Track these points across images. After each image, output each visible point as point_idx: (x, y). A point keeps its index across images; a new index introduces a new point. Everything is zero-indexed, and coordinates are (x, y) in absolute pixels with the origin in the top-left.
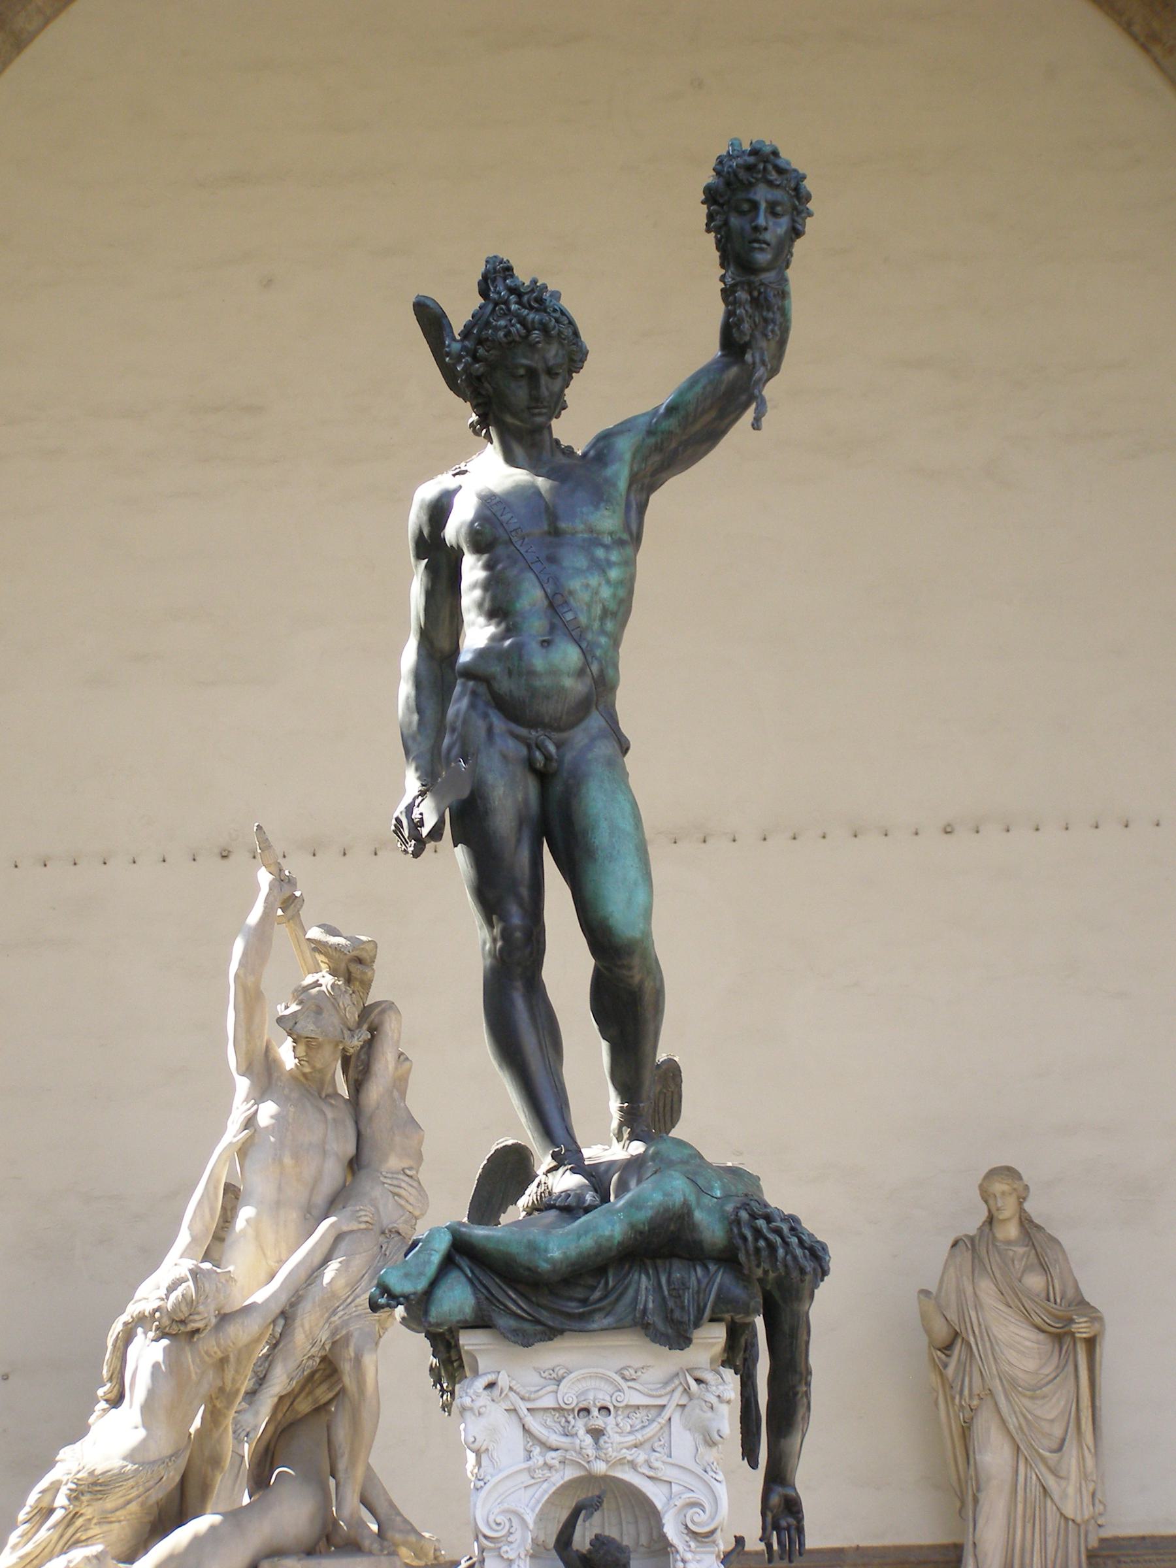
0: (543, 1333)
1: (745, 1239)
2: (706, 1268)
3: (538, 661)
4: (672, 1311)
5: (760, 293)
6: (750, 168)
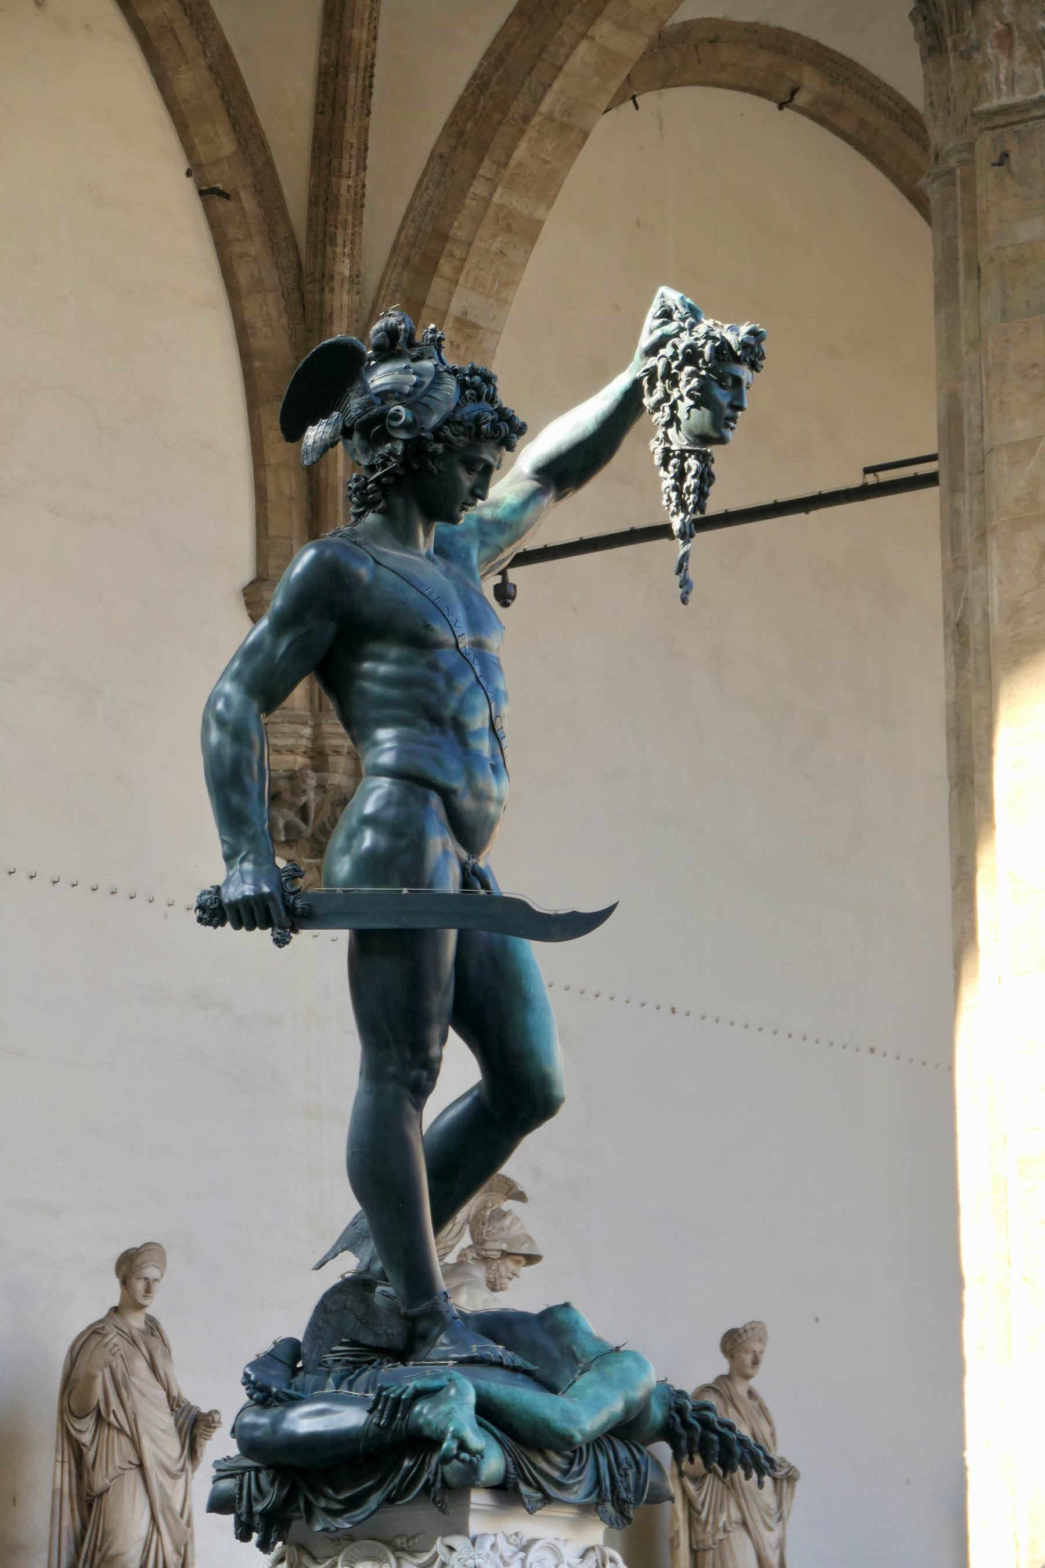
0: (541, 1501)
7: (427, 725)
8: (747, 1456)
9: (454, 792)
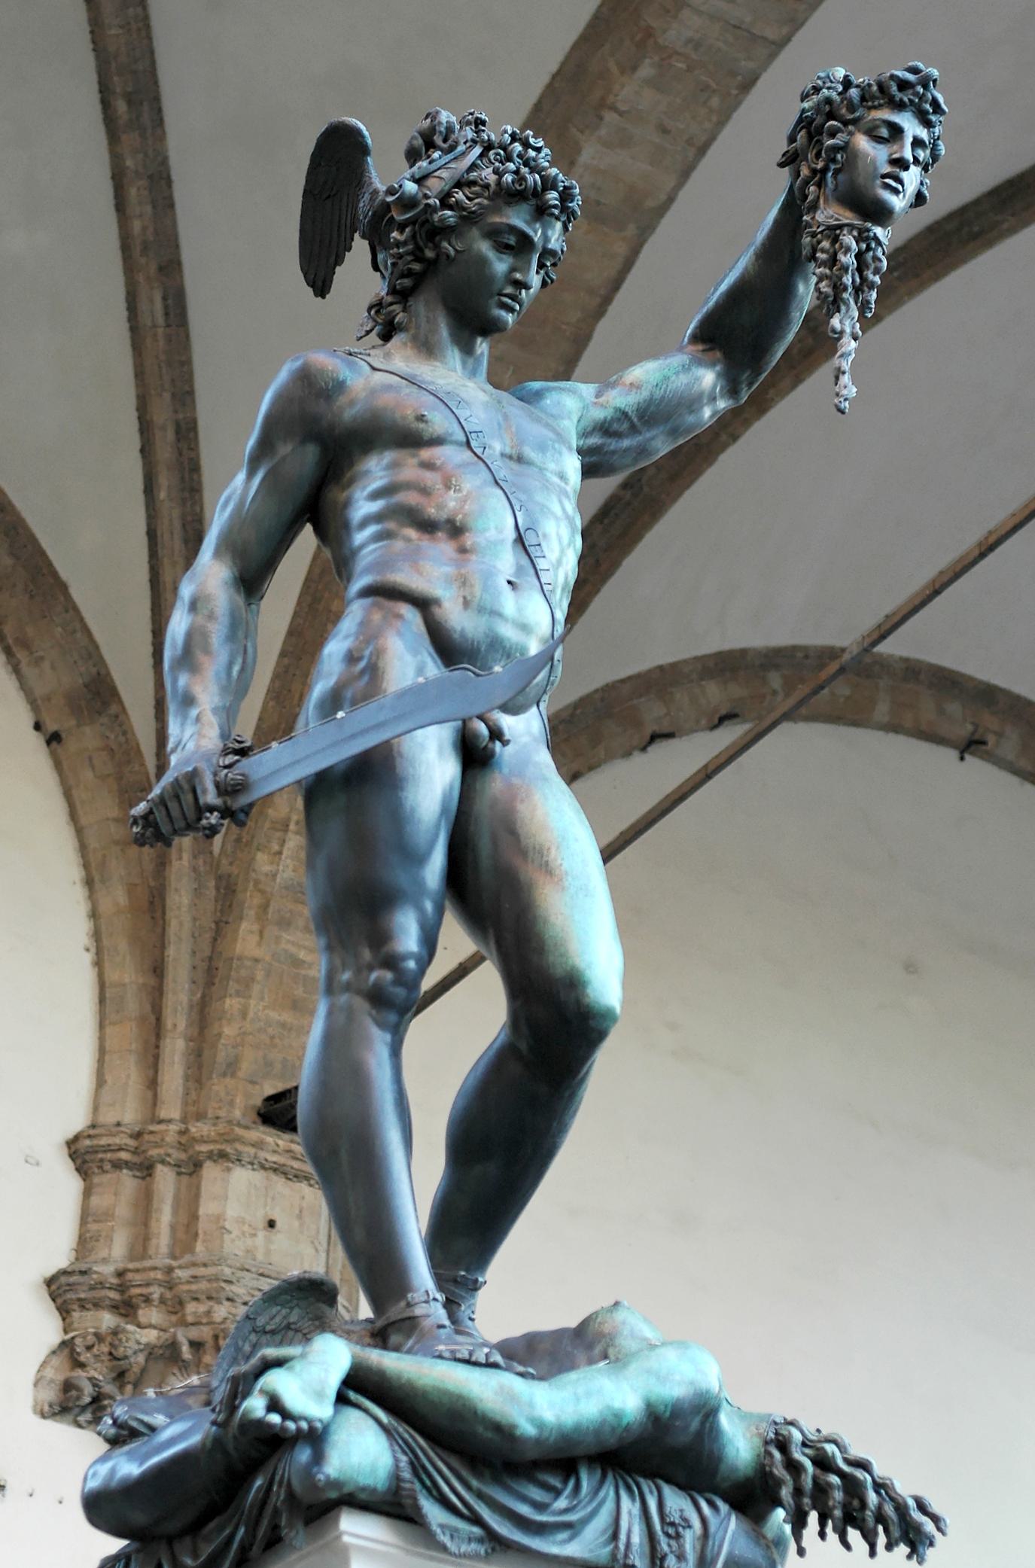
0: (480, 1541)
1: (794, 1467)
2: (712, 1504)
3: (509, 603)
4: (663, 1558)
5: (869, 248)
6: (903, 85)
7: (412, 533)
8: (889, 1509)
9: (436, 602)
